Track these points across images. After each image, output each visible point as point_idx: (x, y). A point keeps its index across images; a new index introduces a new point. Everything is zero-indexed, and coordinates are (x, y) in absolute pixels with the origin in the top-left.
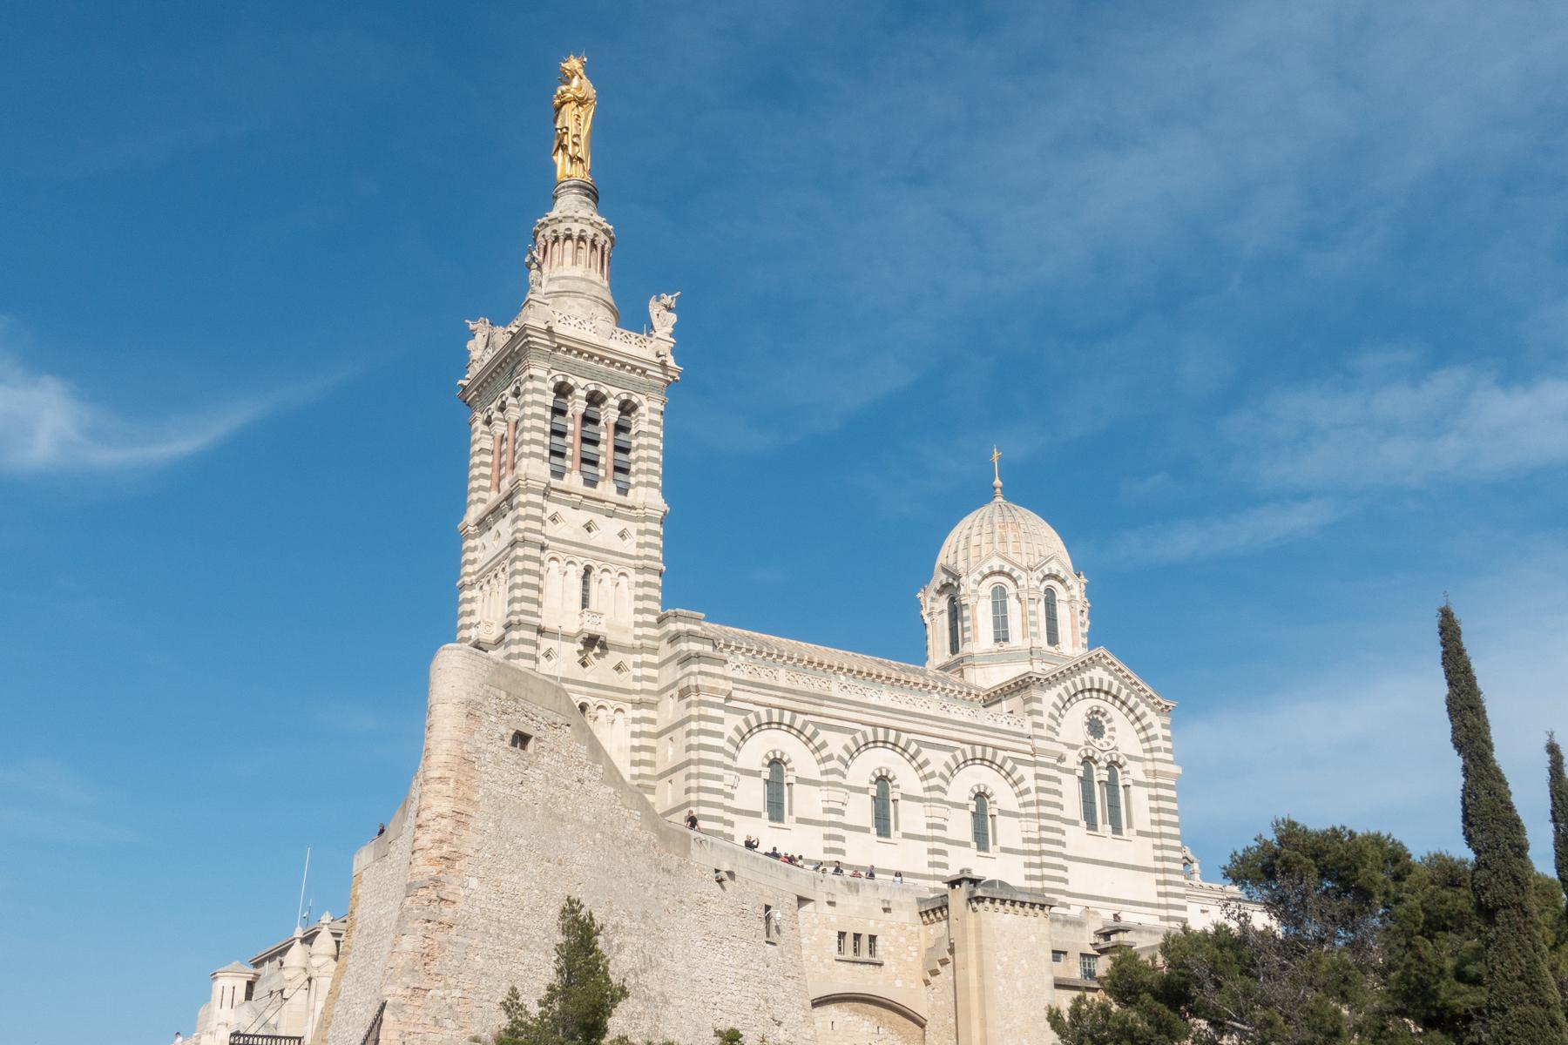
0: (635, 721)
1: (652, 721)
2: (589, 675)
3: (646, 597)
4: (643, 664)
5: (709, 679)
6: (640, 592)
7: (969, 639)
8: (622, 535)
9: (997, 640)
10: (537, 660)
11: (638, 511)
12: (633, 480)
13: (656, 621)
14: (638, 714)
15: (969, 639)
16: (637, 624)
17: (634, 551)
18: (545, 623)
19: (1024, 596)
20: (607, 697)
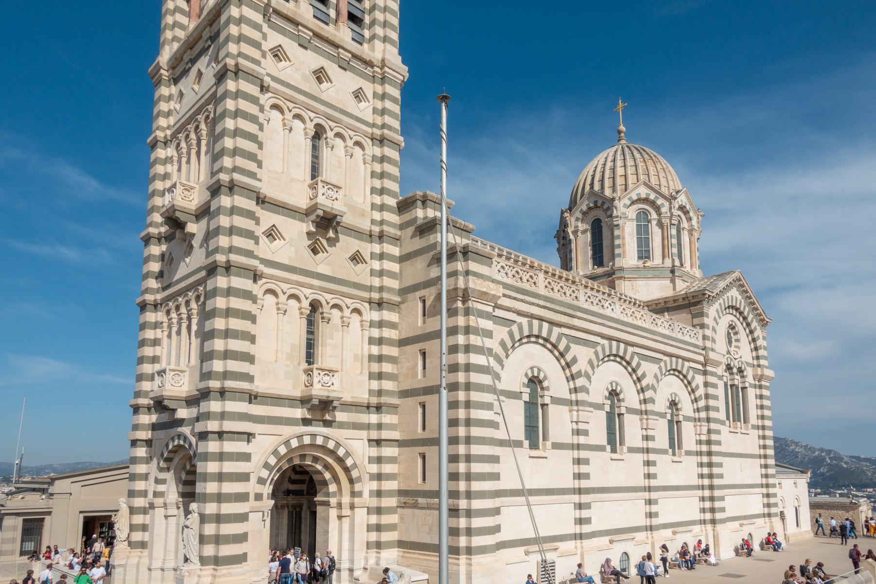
0: (372, 324)
1: (393, 326)
2: (323, 264)
3: (382, 175)
4: (382, 256)
5: (480, 281)
6: (378, 168)
7: (619, 255)
8: (358, 95)
9: (640, 258)
10: (257, 241)
11: (376, 69)
12: (367, 33)
13: (395, 206)
14: (375, 316)
15: (619, 255)
16: (373, 206)
17: (369, 117)
18: (267, 190)
19: (666, 221)
20: (343, 295)
